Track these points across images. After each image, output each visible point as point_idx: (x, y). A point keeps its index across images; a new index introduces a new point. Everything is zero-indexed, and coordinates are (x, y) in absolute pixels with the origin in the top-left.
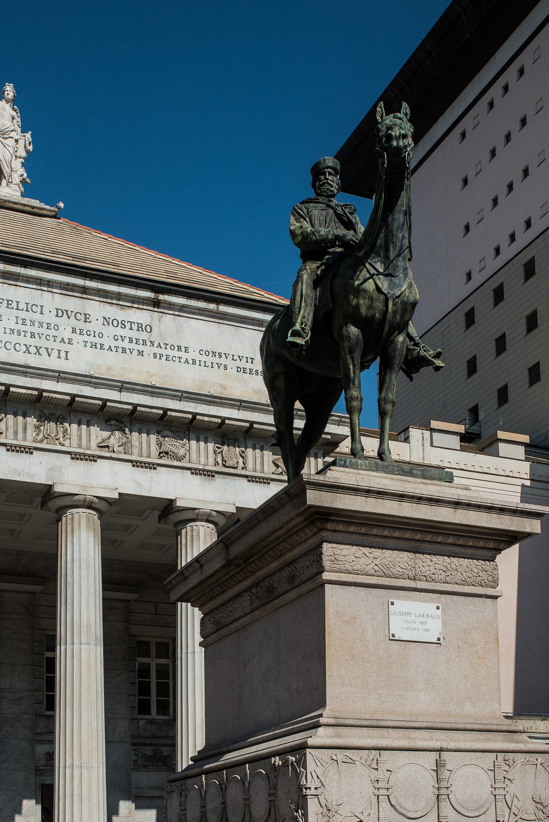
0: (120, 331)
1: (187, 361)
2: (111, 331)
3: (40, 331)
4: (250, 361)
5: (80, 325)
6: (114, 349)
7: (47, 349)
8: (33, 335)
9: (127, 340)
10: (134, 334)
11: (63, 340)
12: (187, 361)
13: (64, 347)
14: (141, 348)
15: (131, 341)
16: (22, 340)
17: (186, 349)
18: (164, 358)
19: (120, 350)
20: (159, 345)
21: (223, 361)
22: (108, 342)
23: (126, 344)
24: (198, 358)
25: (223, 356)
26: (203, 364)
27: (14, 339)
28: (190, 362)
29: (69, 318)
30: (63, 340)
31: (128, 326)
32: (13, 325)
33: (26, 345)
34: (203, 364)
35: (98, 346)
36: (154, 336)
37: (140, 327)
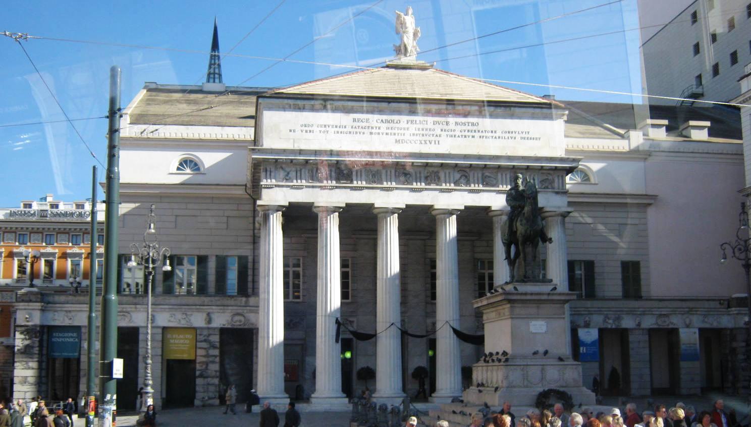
0: (464, 128)
1: (496, 138)
2: (459, 128)
3: (427, 132)
4: (527, 133)
5: (445, 127)
6: (461, 137)
7: (430, 141)
8: (423, 135)
9: (467, 131)
10: (470, 128)
11: (437, 136)
12: (496, 138)
13: (437, 139)
14: (473, 134)
15: (468, 131)
16: (418, 138)
17: (495, 132)
18: (485, 137)
19: (463, 136)
20: (482, 132)
21: (514, 135)
22: (458, 133)
23: (466, 133)
24: (501, 135)
25: (514, 133)
26: (503, 138)
27: (415, 138)
28: (497, 138)
29: (439, 124)
30: (437, 136)
31: (467, 124)
32: (414, 131)
33: (420, 140)
34: (503, 138)
35: (453, 136)
36: (480, 128)
37: (473, 124)
